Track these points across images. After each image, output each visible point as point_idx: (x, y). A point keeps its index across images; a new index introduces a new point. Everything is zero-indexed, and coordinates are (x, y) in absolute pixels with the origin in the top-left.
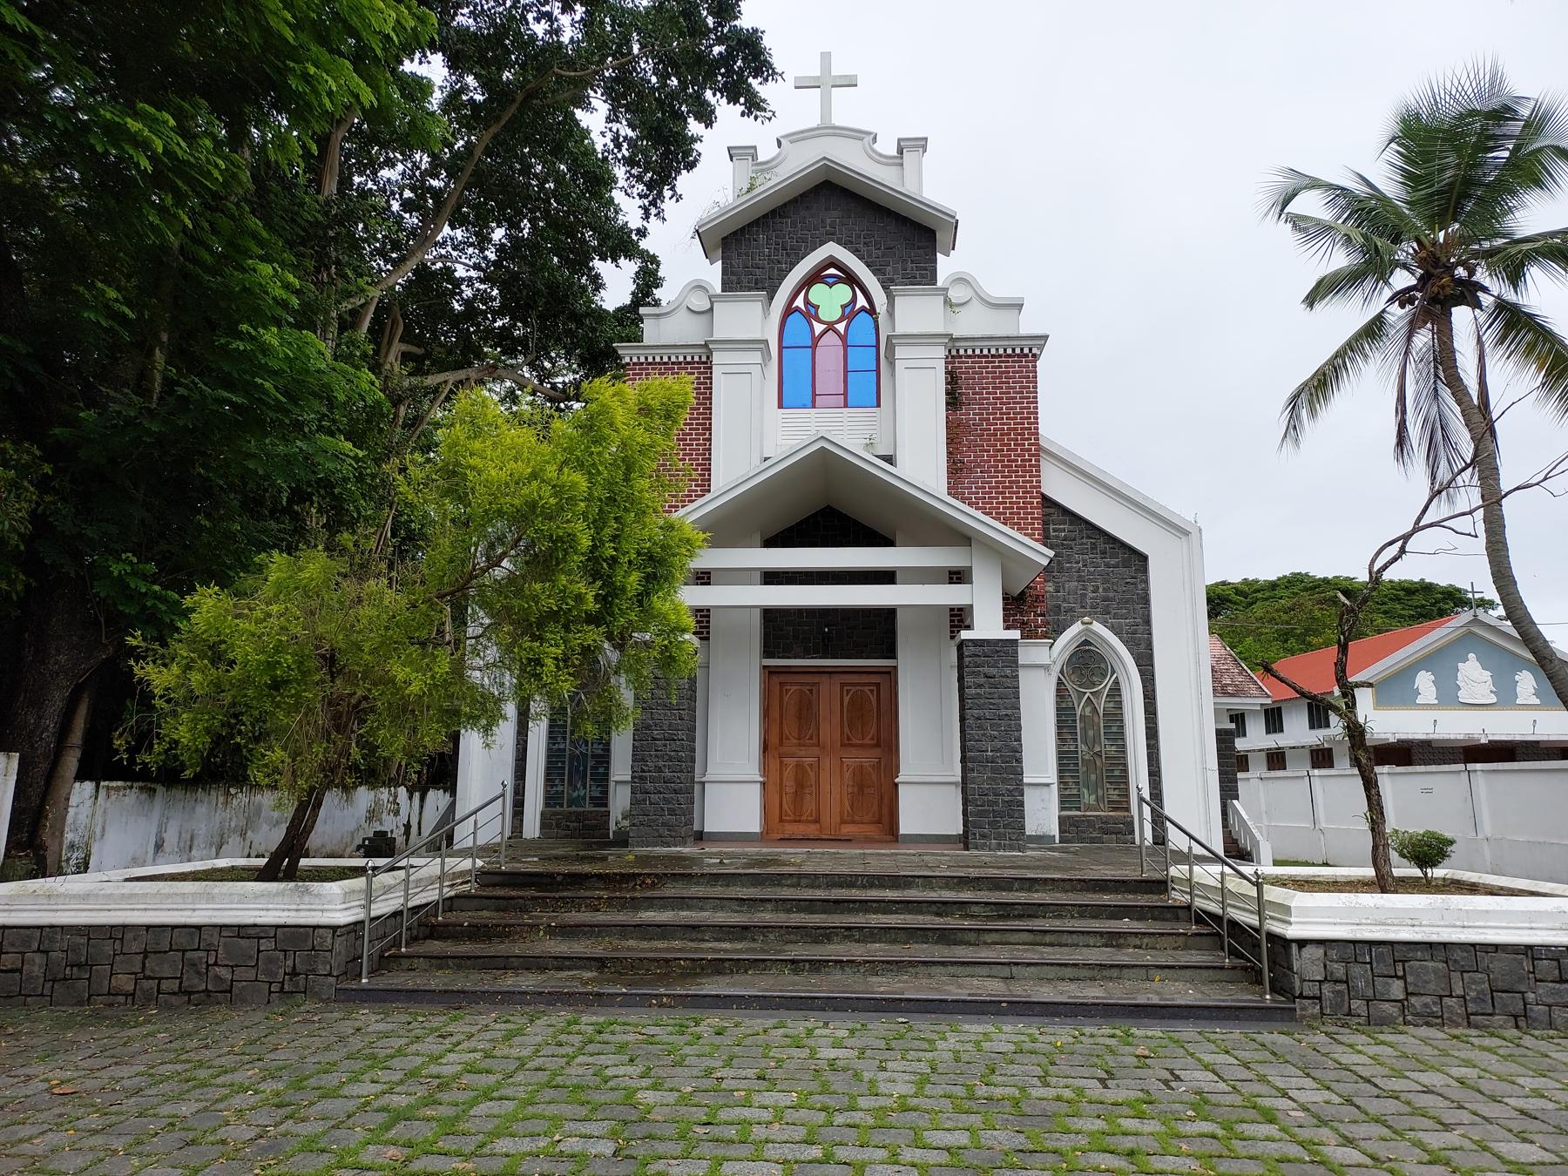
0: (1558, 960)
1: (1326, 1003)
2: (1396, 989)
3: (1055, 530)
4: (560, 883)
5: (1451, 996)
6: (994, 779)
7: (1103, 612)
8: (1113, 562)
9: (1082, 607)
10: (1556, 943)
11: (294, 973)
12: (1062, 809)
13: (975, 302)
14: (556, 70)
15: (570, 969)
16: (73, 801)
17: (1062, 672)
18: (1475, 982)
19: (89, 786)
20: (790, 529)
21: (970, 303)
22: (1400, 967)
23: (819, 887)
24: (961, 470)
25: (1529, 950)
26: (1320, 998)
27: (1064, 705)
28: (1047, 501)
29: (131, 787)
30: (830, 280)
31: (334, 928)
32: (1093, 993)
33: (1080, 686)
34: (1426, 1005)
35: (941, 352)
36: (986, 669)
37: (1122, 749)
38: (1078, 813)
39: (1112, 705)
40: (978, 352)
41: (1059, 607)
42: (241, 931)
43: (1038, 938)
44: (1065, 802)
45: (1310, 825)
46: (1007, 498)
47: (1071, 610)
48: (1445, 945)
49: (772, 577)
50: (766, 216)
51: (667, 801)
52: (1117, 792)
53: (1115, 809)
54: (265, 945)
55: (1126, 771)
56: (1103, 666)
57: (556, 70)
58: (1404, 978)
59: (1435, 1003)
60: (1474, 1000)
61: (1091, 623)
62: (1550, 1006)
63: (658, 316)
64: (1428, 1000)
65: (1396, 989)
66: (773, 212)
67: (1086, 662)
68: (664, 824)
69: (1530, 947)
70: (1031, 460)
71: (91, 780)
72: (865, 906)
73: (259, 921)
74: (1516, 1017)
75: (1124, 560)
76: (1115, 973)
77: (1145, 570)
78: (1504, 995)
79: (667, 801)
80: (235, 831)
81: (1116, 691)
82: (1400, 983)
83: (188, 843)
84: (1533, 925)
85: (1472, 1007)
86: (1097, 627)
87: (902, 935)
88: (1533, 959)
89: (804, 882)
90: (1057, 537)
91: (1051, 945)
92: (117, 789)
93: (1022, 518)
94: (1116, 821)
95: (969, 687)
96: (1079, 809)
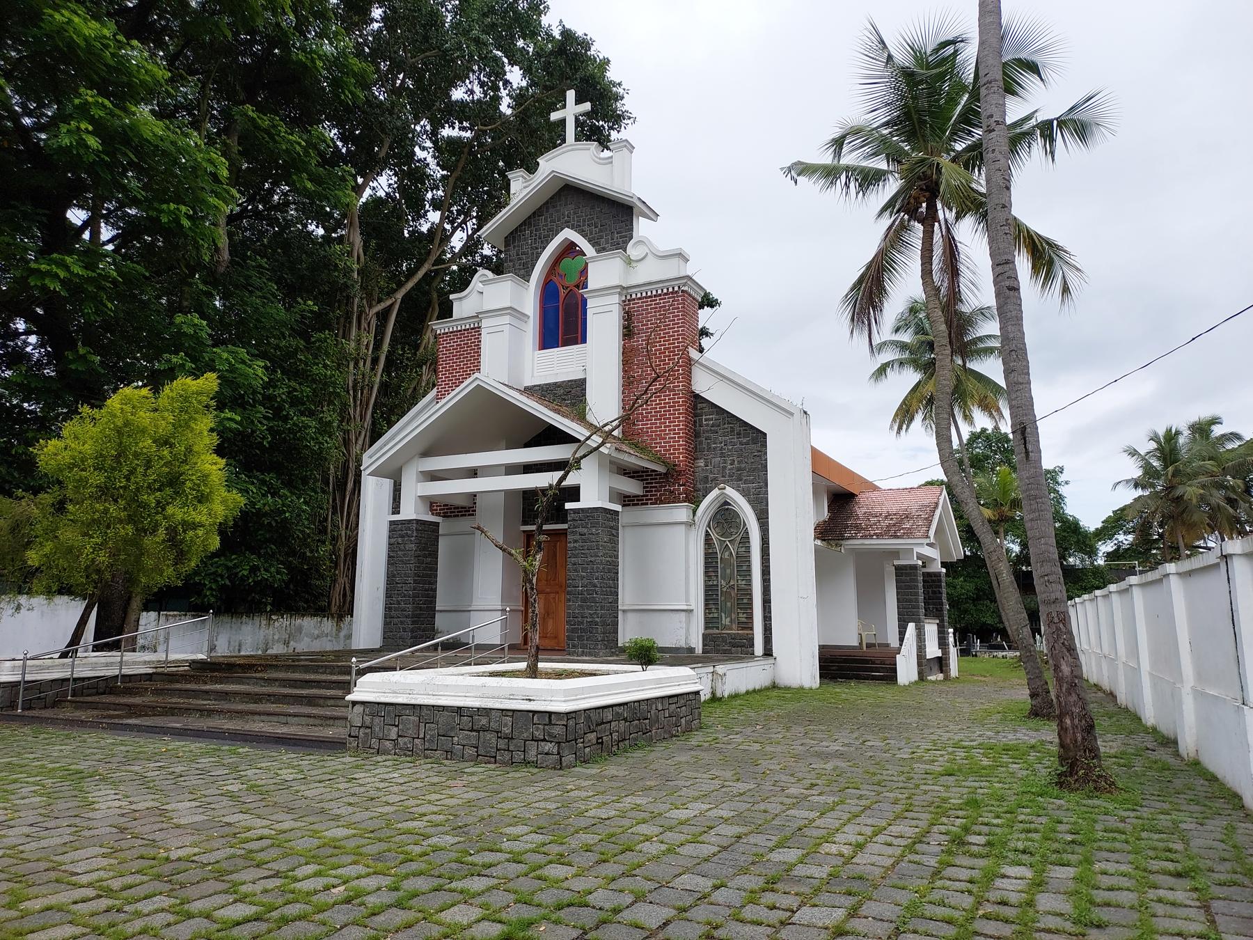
0: (472, 717)
2: (393, 732)
3: (706, 420)
4: (224, 669)
5: (418, 738)
7: (736, 479)
8: (745, 440)
9: (723, 476)
10: (470, 706)
12: (706, 628)
15: (119, 710)
16: (142, 622)
17: (709, 526)
19: (153, 615)
20: (539, 435)
21: (647, 258)
22: (397, 720)
23: (334, 674)
24: (632, 382)
25: (459, 710)
27: (710, 551)
28: (697, 402)
29: (186, 615)
33: (721, 536)
34: (405, 743)
35: (616, 299)
36: (580, 530)
38: (717, 631)
39: (743, 549)
40: (644, 294)
41: (707, 477)
44: (709, 622)
46: (662, 400)
47: (715, 479)
48: (420, 706)
49: (529, 468)
50: (529, 217)
51: (402, 623)
52: (745, 615)
53: (743, 629)
56: (738, 520)
58: (397, 726)
60: (428, 741)
61: (725, 488)
62: (464, 746)
65: (393, 732)
66: (534, 213)
68: (400, 638)
69: (460, 708)
70: (679, 370)
74: (447, 752)
75: (753, 439)
76: (331, 722)
77: (765, 445)
78: (443, 738)
79: (402, 623)
80: (278, 641)
81: (746, 539)
82: (396, 729)
83: (237, 648)
84: (467, 695)
86: (731, 492)
88: (461, 716)
89: (328, 671)
90: (707, 425)
92: (175, 616)
93: (672, 414)
94: (742, 637)
95: (570, 542)
96: (718, 628)
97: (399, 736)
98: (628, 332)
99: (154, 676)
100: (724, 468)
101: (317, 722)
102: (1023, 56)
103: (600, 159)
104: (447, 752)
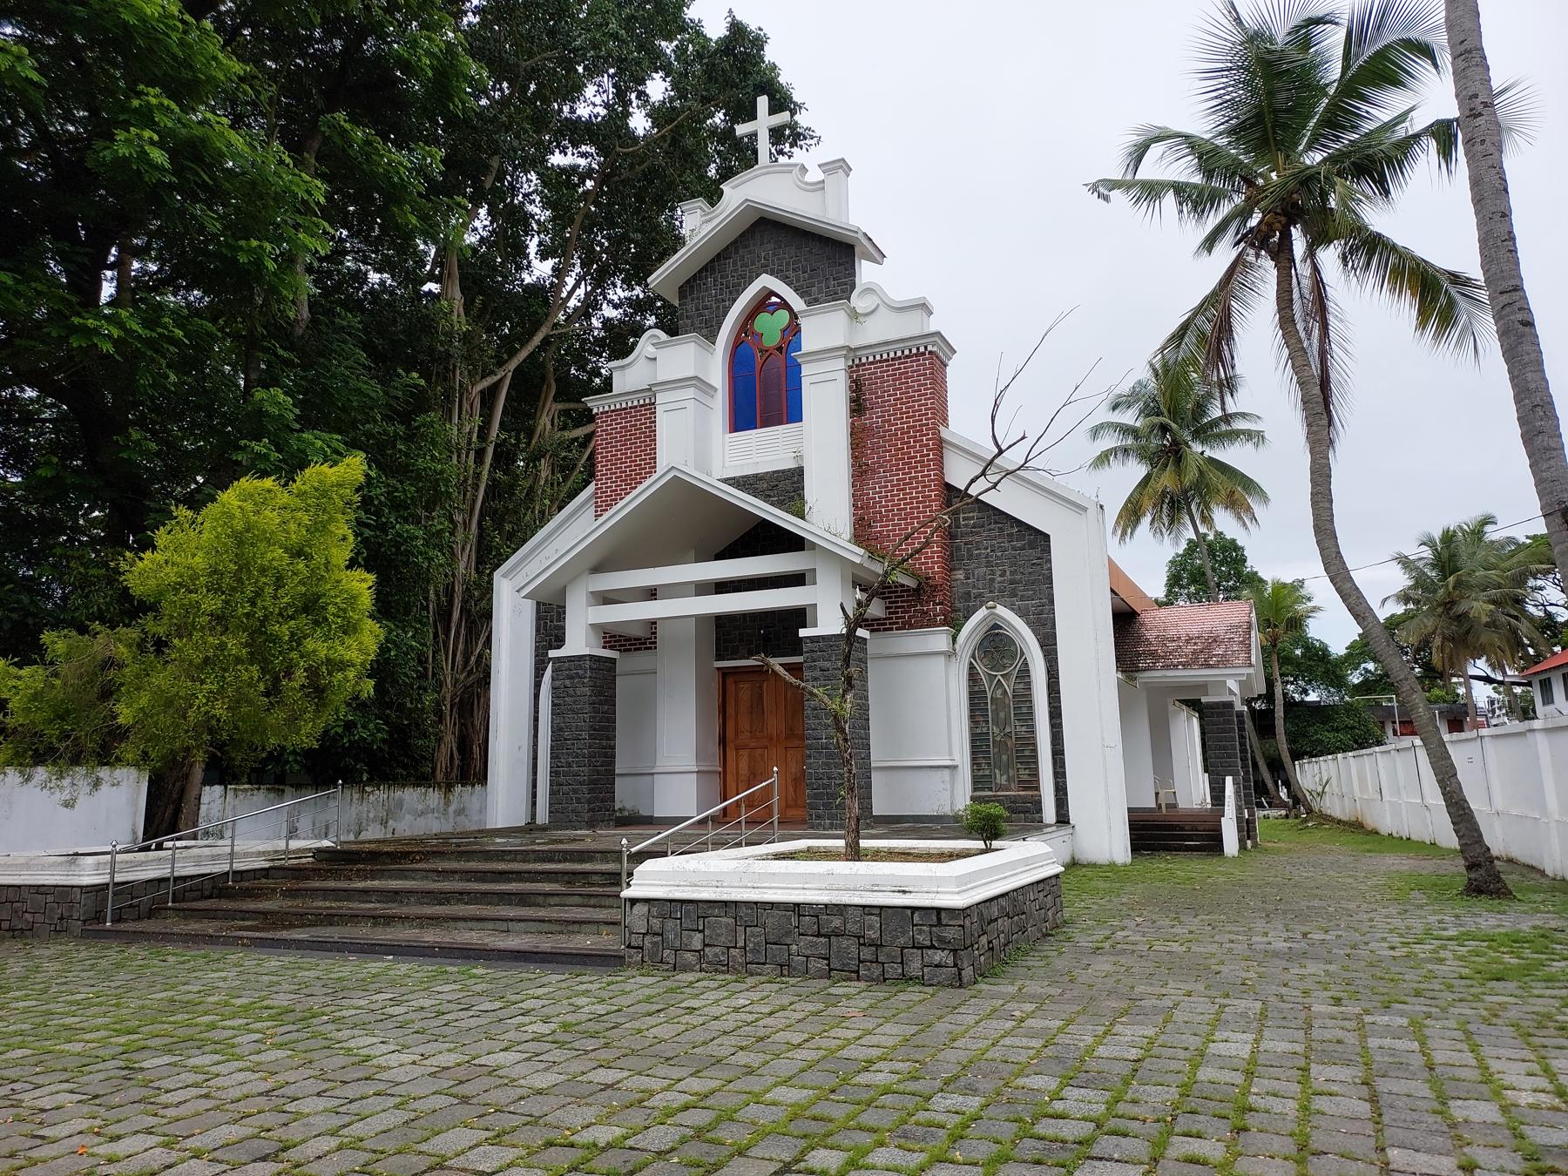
1: (646, 952)
2: (697, 941)
3: (964, 519)
5: (735, 947)
6: (827, 764)
7: (1009, 595)
9: (991, 592)
11: (61, 918)
12: (975, 790)
13: (882, 308)
14: (618, 149)
16: (204, 799)
17: (973, 656)
18: (753, 935)
19: (218, 789)
20: (735, 543)
22: (701, 922)
23: (529, 862)
24: (866, 472)
26: (642, 948)
27: (976, 689)
30: (771, 308)
31: (81, 887)
32: (546, 944)
33: (991, 669)
34: (716, 955)
36: (821, 664)
37: (1032, 729)
39: (1022, 686)
40: (878, 357)
42: (39, 889)
43: (586, 901)
44: (978, 782)
45: (1419, 801)
47: (980, 595)
48: (736, 903)
49: (723, 587)
50: (712, 261)
51: (575, 791)
52: (1027, 772)
53: (1025, 789)
54: (50, 899)
55: (1035, 751)
57: (618, 149)
58: (702, 931)
59: (723, 953)
60: (752, 951)
63: (623, 367)
64: (717, 950)
65: (697, 941)
66: (719, 255)
67: (996, 645)
69: (798, 905)
71: (220, 784)
72: (519, 876)
73: (46, 882)
74: (781, 966)
75: (1030, 542)
76: (576, 927)
79: (575, 791)
81: (1025, 673)
82: (699, 936)
85: (750, 957)
86: (1001, 610)
87: (496, 899)
88: (799, 916)
89: (519, 857)
90: (966, 526)
91: (594, 906)
92: (246, 790)
94: (1024, 800)
96: (991, 790)
97: (705, 945)
98: (857, 406)
99: (271, 872)
100: (992, 580)
101: (558, 928)
102: (1413, 35)
103: (806, 183)
104: (781, 966)
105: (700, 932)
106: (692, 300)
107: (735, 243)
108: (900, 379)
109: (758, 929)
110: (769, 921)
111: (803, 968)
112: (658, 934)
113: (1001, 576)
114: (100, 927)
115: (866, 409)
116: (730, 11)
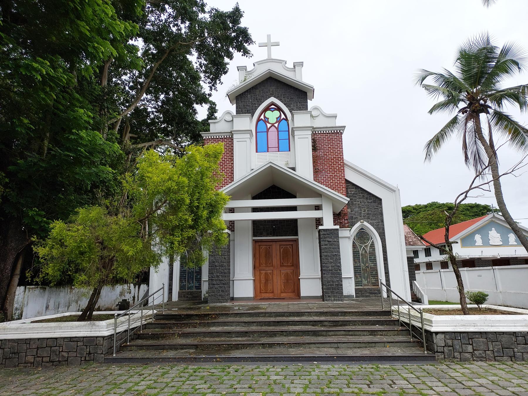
0: (524, 337)
1: (446, 354)
2: (470, 348)
3: (350, 191)
4: (183, 318)
5: (488, 350)
6: (332, 277)
7: (367, 218)
8: (370, 201)
10: (523, 331)
11: (90, 353)
12: (356, 286)
13: (321, 116)
14: (180, 42)
15: (186, 349)
16: (17, 293)
17: (354, 239)
18: (496, 345)
19: (22, 288)
20: (261, 193)
21: (318, 117)
22: (470, 341)
23: (272, 317)
25: (514, 333)
26: (444, 352)
27: (355, 250)
28: (347, 181)
29: (37, 288)
30: (272, 110)
31: (103, 337)
32: (366, 352)
34: (480, 354)
35: (310, 133)
36: (328, 239)
37: (376, 265)
38: (361, 287)
39: (371, 250)
41: (352, 217)
42: (71, 339)
43: (347, 333)
44: (357, 283)
45: (441, 288)
46: (334, 181)
47: (357, 218)
48: (486, 333)
49: (255, 210)
50: (250, 89)
51: (221, 287)
52: (374, 280)
53: (374, 286)
54: (79, 344)
55: (377, 272)
56: (368, 237)
57: (180, 42)
58: (472, 344)
59: (483, 353)
60: (497, 352)
61: (363, 222)
62: (522, 353)
63: (215, 123)
64: (481, 352)
65: (470, 348)
66: (253, 87)
67: (362, 235)
68: (220, 295)
69: (515, 333)
70: (341, 168)
71: (23, 285)
72: (288, 323)
73: (77, 335)
74: (511, 357)
76: (373, 345)
77: (381, 204)
78: (507, 349)
79: (221, 287)
80: (74, 301)
81: (373, 245)
82: (471, 346)
83: (57, 306)
84: (516, 325)
85: (496, 354)
86: (366, 223)
87: (301, 334)
88: (516, 337)
89: (267, 315)
90: (351, 193)
91: (352, 335)
92: (32, 288)
93: (339, 187)
95: (323, 245)
96: (361, 286)
97: (474, 350)
98: (315, 148)
99: (147, 326)
100: (361, 213)
101: (367, 345)
102: (514, 59)
104: (511, 357)
105: (470, 344)
106: (242, 102)
107: (260, 84)
108: (330, 140)
109: (497, 343)
110: (503, 339)
111: (521, 357)
112: (450, 346)
113: (364, 211)
114: (110, 357)
115: (317, 149)
116: (237, 3)
